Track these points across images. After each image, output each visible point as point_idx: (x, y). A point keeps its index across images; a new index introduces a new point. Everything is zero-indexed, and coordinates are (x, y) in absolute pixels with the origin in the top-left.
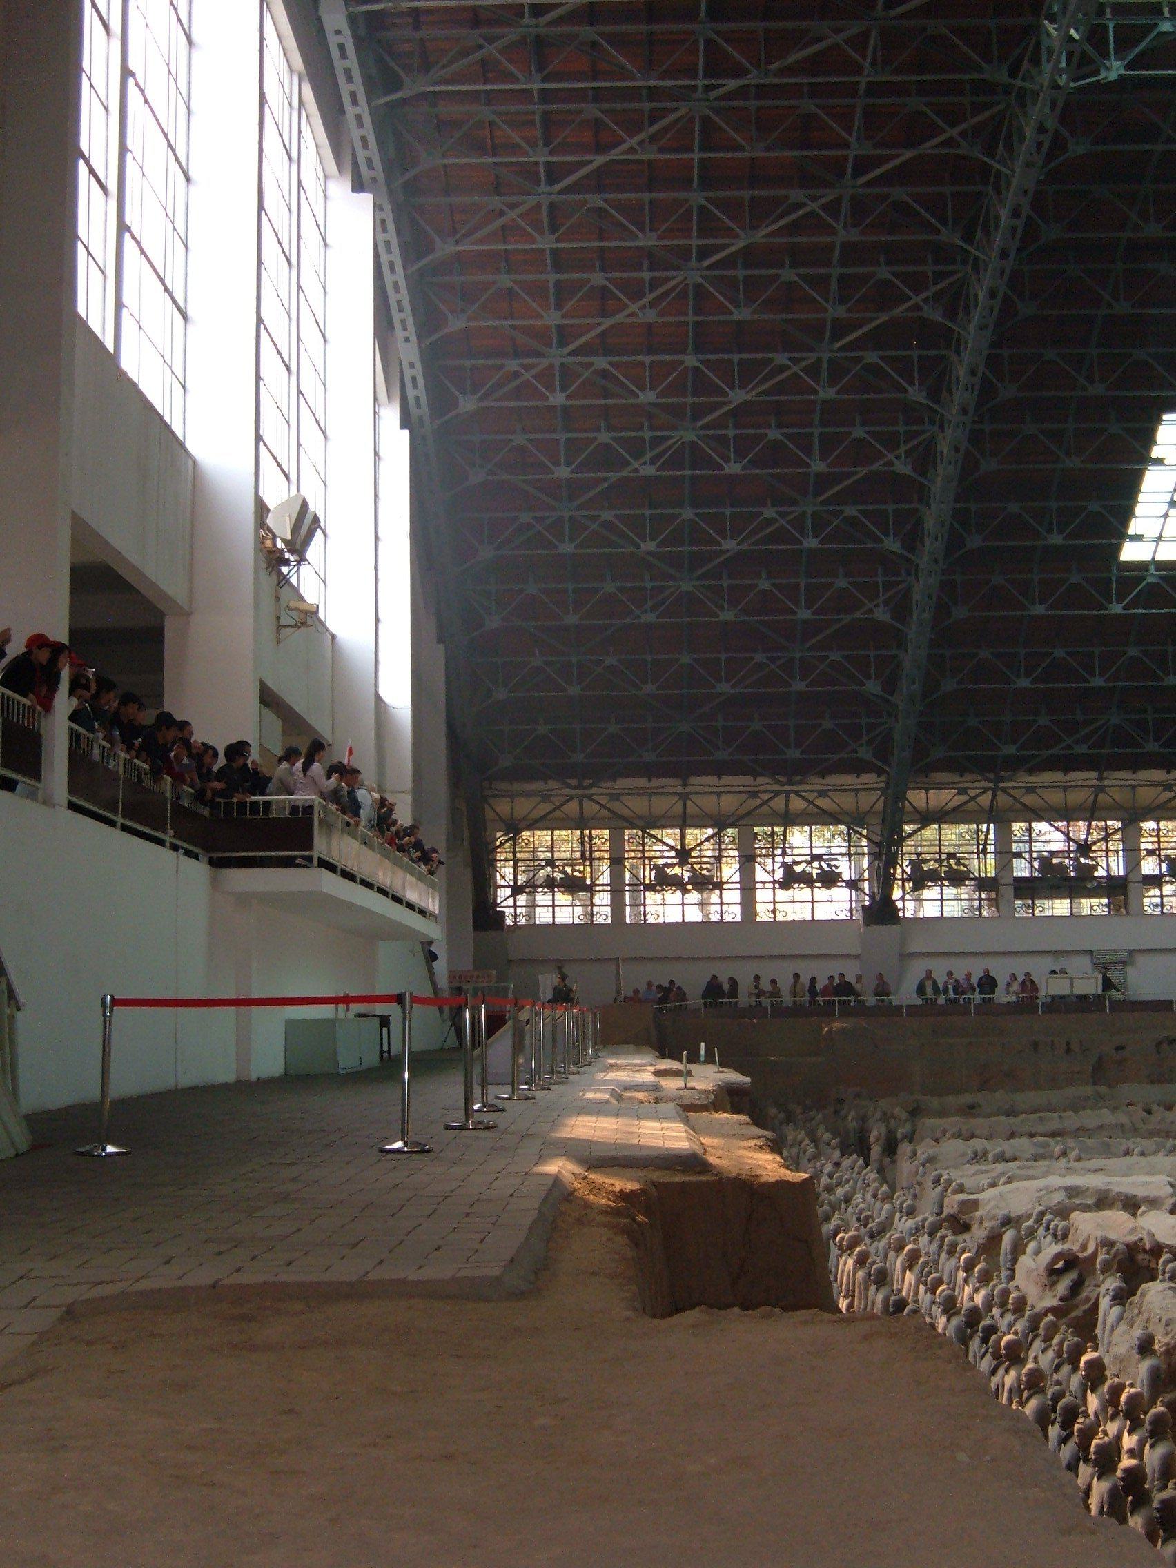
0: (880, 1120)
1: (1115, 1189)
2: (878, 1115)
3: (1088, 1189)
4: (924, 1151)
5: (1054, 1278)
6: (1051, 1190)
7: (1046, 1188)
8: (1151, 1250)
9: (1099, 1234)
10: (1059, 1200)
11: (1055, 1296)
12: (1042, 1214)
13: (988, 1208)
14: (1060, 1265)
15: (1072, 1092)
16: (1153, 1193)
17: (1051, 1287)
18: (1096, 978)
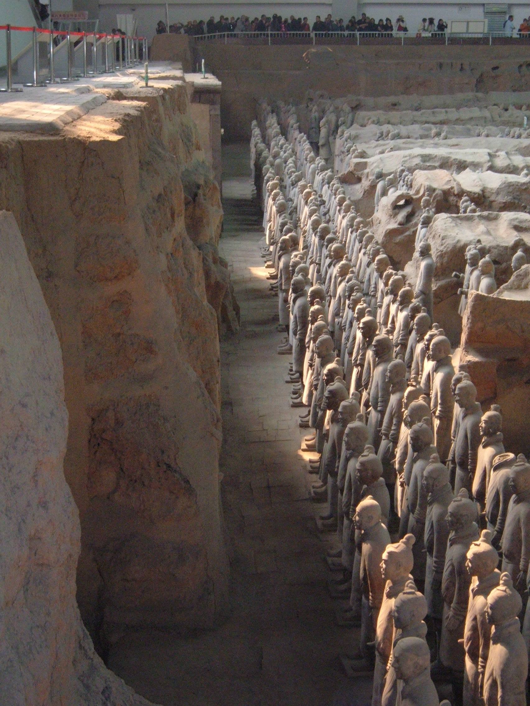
0: (333, 112)
1: (453, 157)
2: (332, 109)
3: (436, 156)
4: (353, 131)
5: (397, 211)
6: (412, 157)
7: (410, 155)
8: (458, 194)
9: (427, 183)
10: (417, 163)
11: (396, 222)
12: (403, 171)
13: (372, 168)
14: (402, 202)
15: (460, 96)
16: (477, 160)
17: (394, 217)
18: (484, 22)
